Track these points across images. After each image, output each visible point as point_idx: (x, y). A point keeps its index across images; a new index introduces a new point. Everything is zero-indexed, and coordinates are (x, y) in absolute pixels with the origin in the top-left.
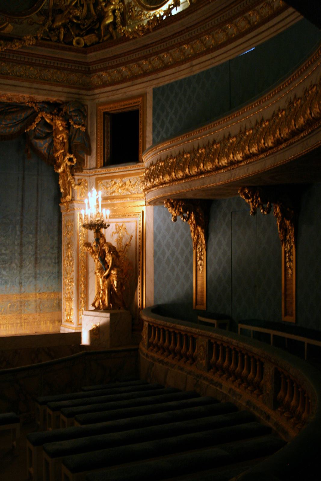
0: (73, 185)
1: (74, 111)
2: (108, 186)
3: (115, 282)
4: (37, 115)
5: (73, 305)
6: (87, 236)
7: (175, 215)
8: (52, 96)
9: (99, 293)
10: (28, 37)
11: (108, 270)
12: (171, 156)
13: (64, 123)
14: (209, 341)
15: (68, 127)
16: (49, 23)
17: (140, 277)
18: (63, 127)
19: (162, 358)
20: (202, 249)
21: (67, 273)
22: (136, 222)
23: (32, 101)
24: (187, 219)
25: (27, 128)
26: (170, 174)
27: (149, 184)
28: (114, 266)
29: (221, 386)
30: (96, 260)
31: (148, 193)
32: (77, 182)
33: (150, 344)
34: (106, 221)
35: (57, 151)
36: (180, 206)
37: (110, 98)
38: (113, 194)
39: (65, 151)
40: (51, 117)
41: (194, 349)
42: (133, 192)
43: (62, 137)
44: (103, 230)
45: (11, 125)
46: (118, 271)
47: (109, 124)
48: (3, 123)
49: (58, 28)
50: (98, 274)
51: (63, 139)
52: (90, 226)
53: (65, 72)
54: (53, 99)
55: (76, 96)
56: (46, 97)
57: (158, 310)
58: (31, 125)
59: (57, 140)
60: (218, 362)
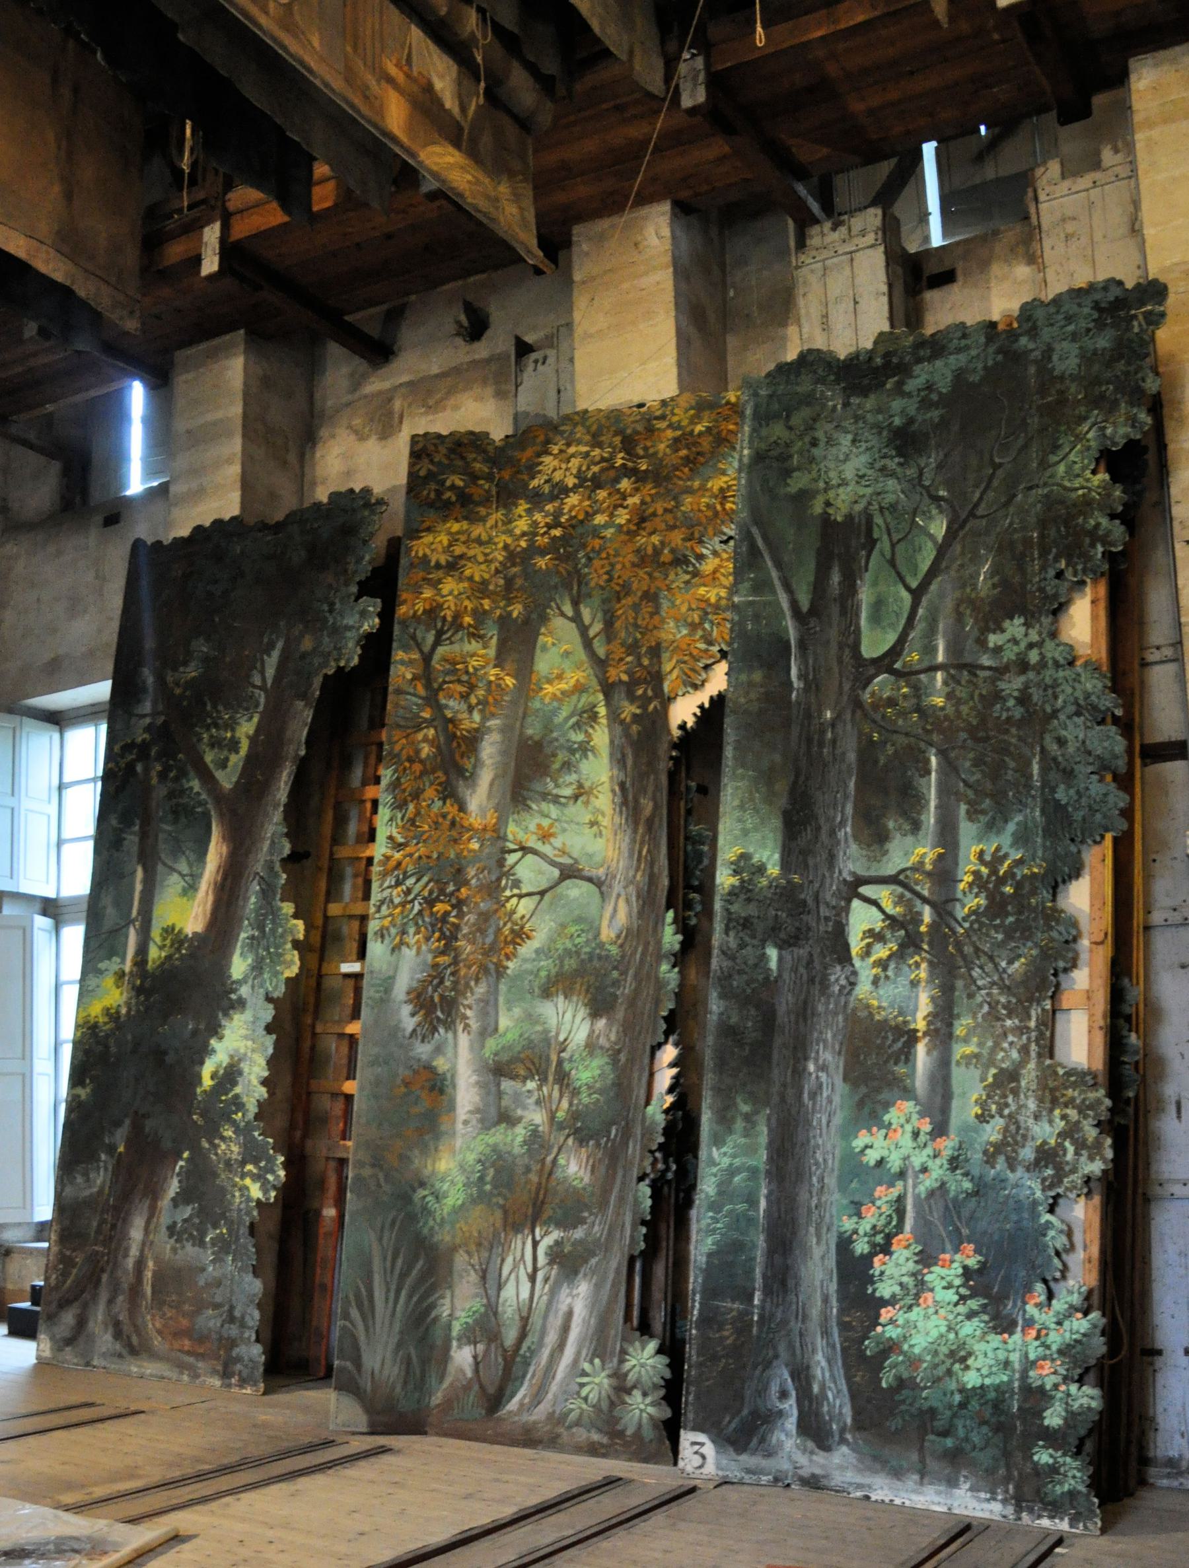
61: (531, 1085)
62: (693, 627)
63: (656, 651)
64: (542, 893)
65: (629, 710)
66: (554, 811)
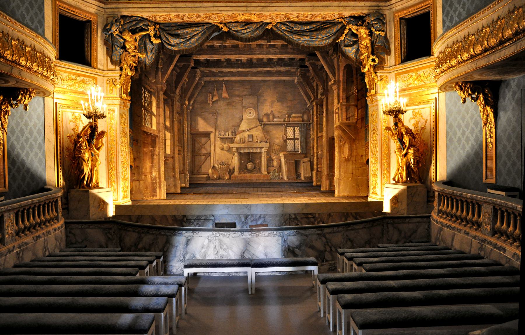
2: (405, 79)
3: (412, 160)
5: (378, 179)
6: (389, 123)
7: (464, 97)
8: (357, 10)
9: (399, 169)
11: (406, 150)
12: (457, 41)
13: (367, 31)
14: (494, 207)
15: (371, 34)
17: (434, 155)
18: (366, 34)
19: (449, 223)
20: (491, 128)
22: (431, 107)
24: (476, 99)
25: (338, 39)
26: (456, 57)
27: (438, 71)
28: (411, 146)
29: (505, 250)
30: (396, 141)
31: (438, 78)
32: (379, 78)
33: (440, 211)
34: (404, 109)
35: (362, 54)
36: (468, 88)
37: (405, 5)
38: (410, 86)
40: (356, 28)
41: (479, 216)
42: (427, 82)
43: (366, 42)
44: (401, 116)
46: (414, 150)
47: (405, 27)
48: (320, 37)
50: (398, 153)
52: (390, 112)
55: (376, 8)
56: (352, 12)
57: (449, 182)
59: (362, 46)
60: (503, 227)
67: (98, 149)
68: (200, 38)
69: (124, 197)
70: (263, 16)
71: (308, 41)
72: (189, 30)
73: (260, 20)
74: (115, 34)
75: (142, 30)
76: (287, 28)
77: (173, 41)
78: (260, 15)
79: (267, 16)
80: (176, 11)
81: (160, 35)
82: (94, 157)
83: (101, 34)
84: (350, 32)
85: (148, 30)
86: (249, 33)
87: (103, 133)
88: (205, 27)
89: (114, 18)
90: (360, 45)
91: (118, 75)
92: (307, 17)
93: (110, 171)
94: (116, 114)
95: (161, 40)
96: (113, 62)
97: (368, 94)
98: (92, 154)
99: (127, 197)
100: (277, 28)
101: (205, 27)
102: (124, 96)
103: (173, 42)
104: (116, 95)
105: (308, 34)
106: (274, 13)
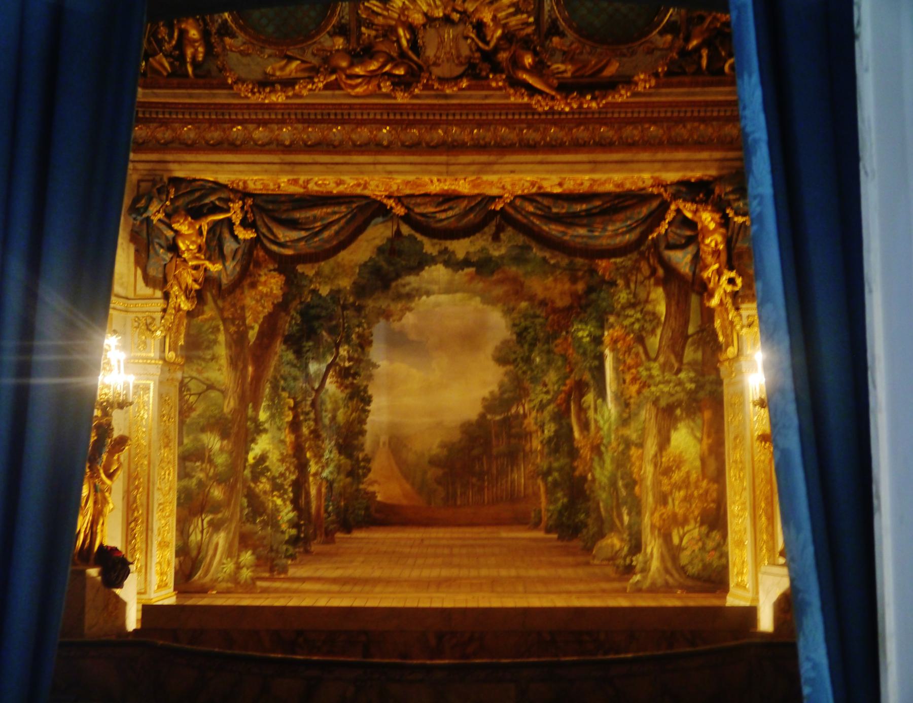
0: (738, 327)
1: (732, 192)
4: (668, 208)
5: (748, 554)
8: (692, 170)
10: (642, 76)
15: (725, 222)
16: (680, 43)
18: (715, 222)
21: (735, 494)
23: (659, 183)
25: (652, 232)
32: (745, 322)
35: (706, 267)
39: (720, 267)
43: (714, 241)
45: (624, 229)
49: (697, 49)
51: (716, 245)
53: (715, 123)
54: (695, 175)
58: (659, 225)
59: (706, 248)
61: (198, 464)
62: (257, 301)
63: (243, 308)
64: (200, 394)
65: (233, 329)
66: (203, 364)
67: (110, 476)
68: (342, 228)
69: (159, 587)
70: (487, 182)
71: (582, 237)
72: (318, 212)
73: (476, 191)
74: (155, 220)
75: (215, 210)
76: (536, 208)
77: (284, 235)
78: (475, 185)
79: (491, 184)
80: (292, 172)
81: (254, 222)
82: (99, 495)
83: (126, 220)
84: (680, 217)
85: (228, 210)
86: (453, 219)
87: (122, 441)
88: (354, 206)
89: (154, 185)
90: (702, 246)
91: (159, 309)
92: (582, 184)
93: (133, 525)
94: (151, 397)
95: (256, 231)
96: (148, 280)
97: (722, 357)
98: (95, 486)
99: (166, 585)
100: (515, 208)
101: (354, 206)
102: (171, 355)
103: (284, 236)
104: (152, 355)
105: (585, 221)
106: (507, 179)
